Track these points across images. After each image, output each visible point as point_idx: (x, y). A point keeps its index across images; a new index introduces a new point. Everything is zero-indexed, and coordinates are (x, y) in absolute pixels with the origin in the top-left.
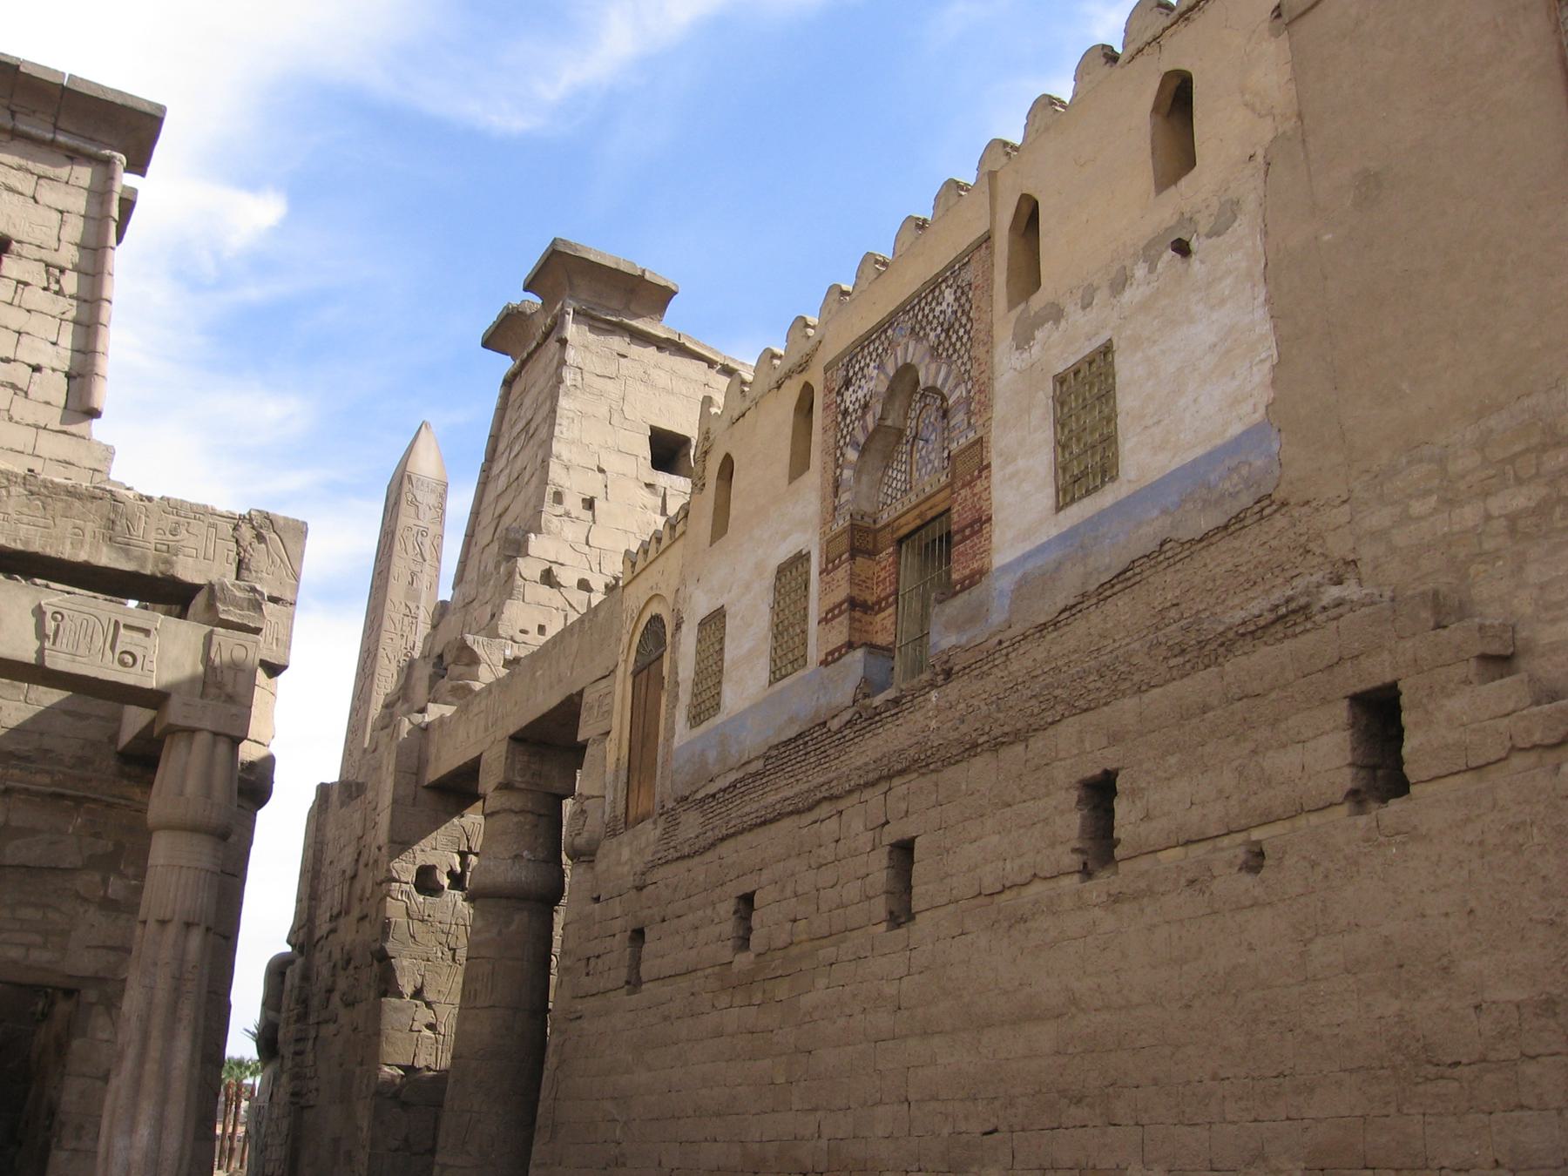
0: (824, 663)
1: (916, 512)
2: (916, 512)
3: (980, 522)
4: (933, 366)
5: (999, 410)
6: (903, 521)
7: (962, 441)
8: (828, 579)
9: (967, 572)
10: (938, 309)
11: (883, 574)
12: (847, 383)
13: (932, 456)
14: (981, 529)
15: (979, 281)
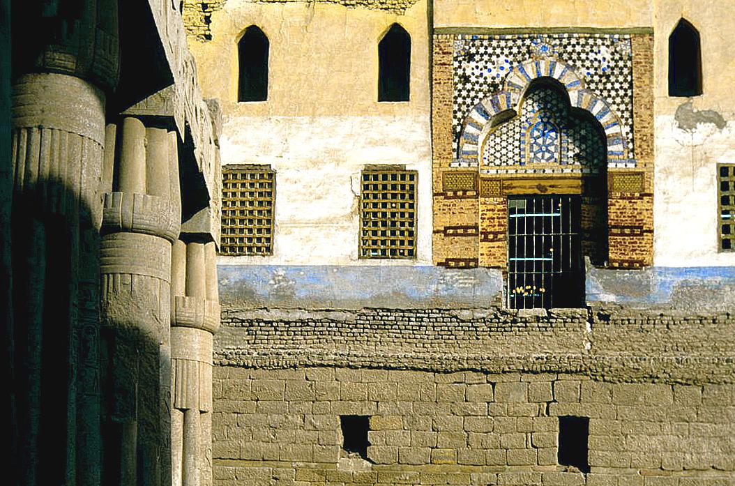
0: (445, 265)
1: (536, 183)
2: (536, 183)
3: (640, 230)
4: (587, 97)
5: (660, 160)
6: (515, 183)
7: (620, 165)
8: (448, 202)
9: (627, 258)
10: (592, 56)
11: (490, 214)
12: (470, 57)
13: (552, 148)
14: (641, 234)
15: (641, 58)
